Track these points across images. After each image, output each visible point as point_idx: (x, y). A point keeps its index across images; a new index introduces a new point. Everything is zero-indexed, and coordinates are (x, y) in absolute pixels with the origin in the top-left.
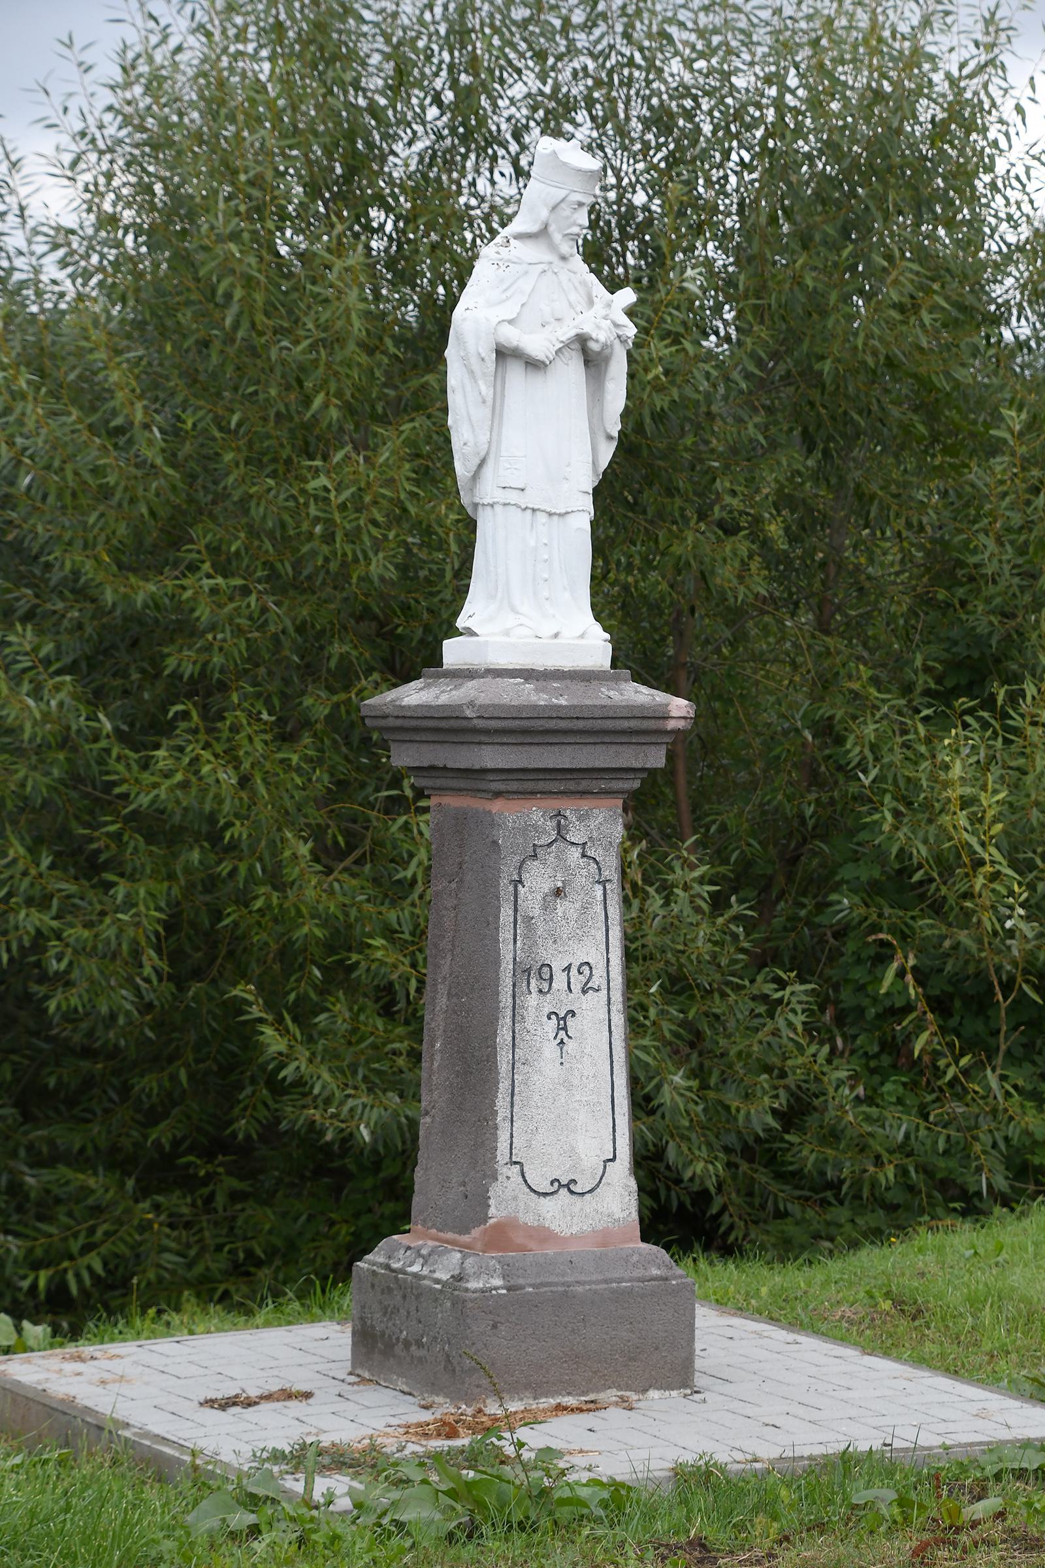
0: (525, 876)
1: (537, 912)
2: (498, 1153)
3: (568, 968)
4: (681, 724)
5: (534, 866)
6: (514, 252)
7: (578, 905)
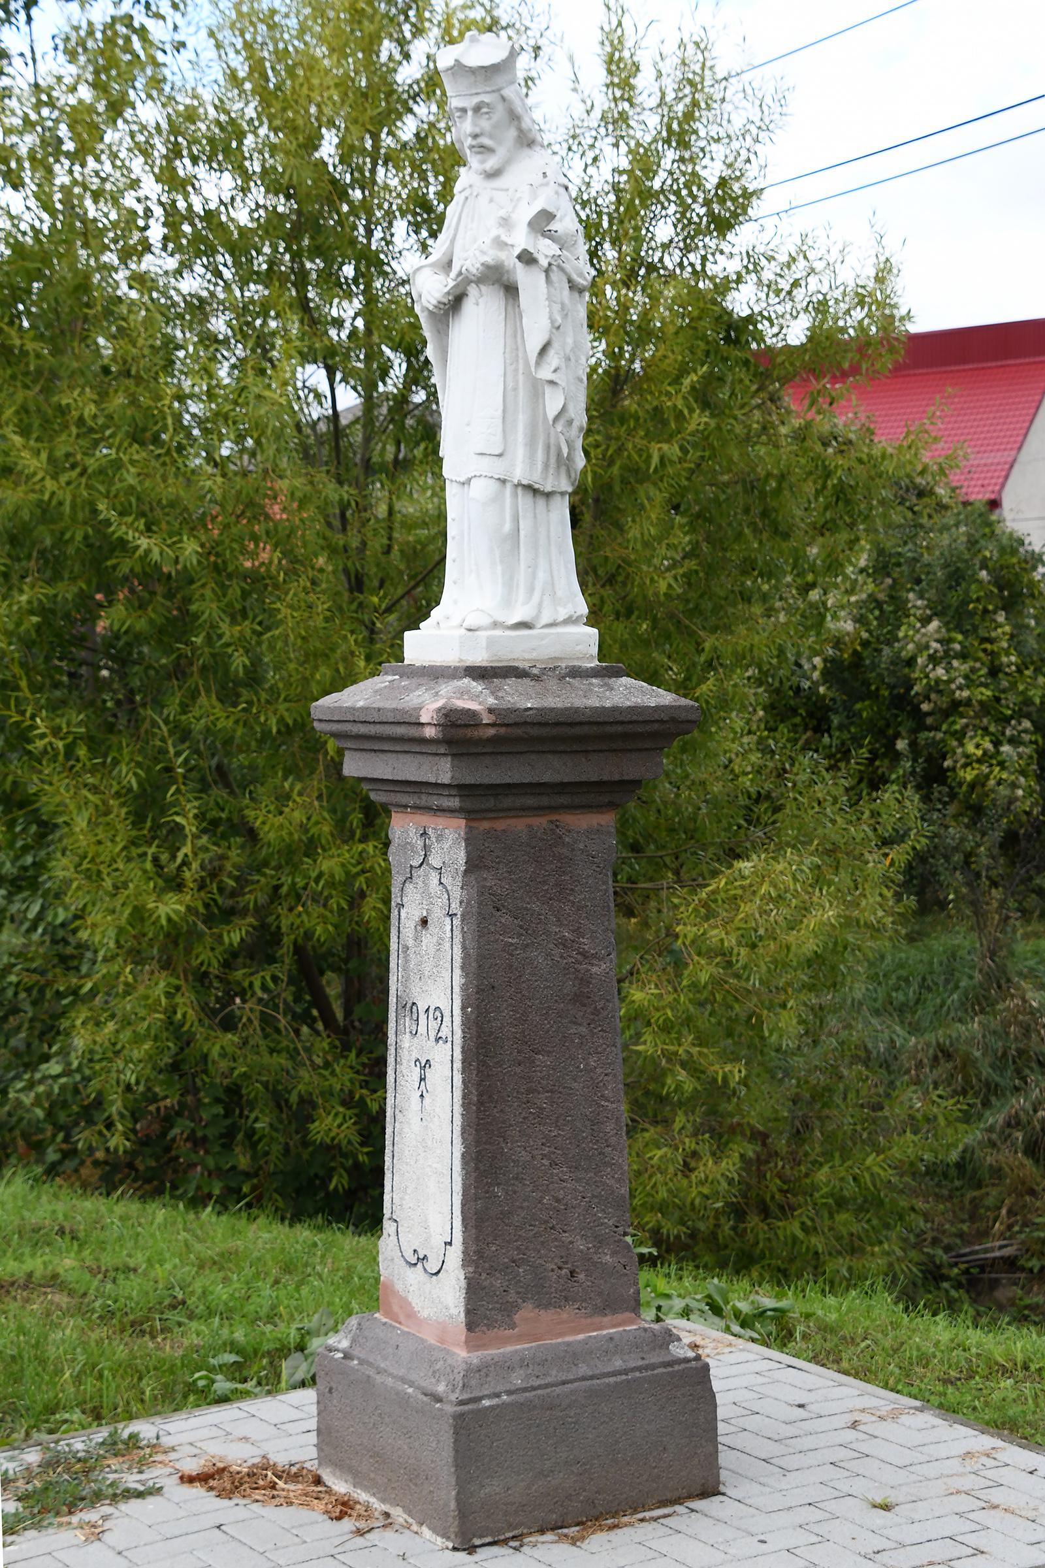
5: (409, 887)
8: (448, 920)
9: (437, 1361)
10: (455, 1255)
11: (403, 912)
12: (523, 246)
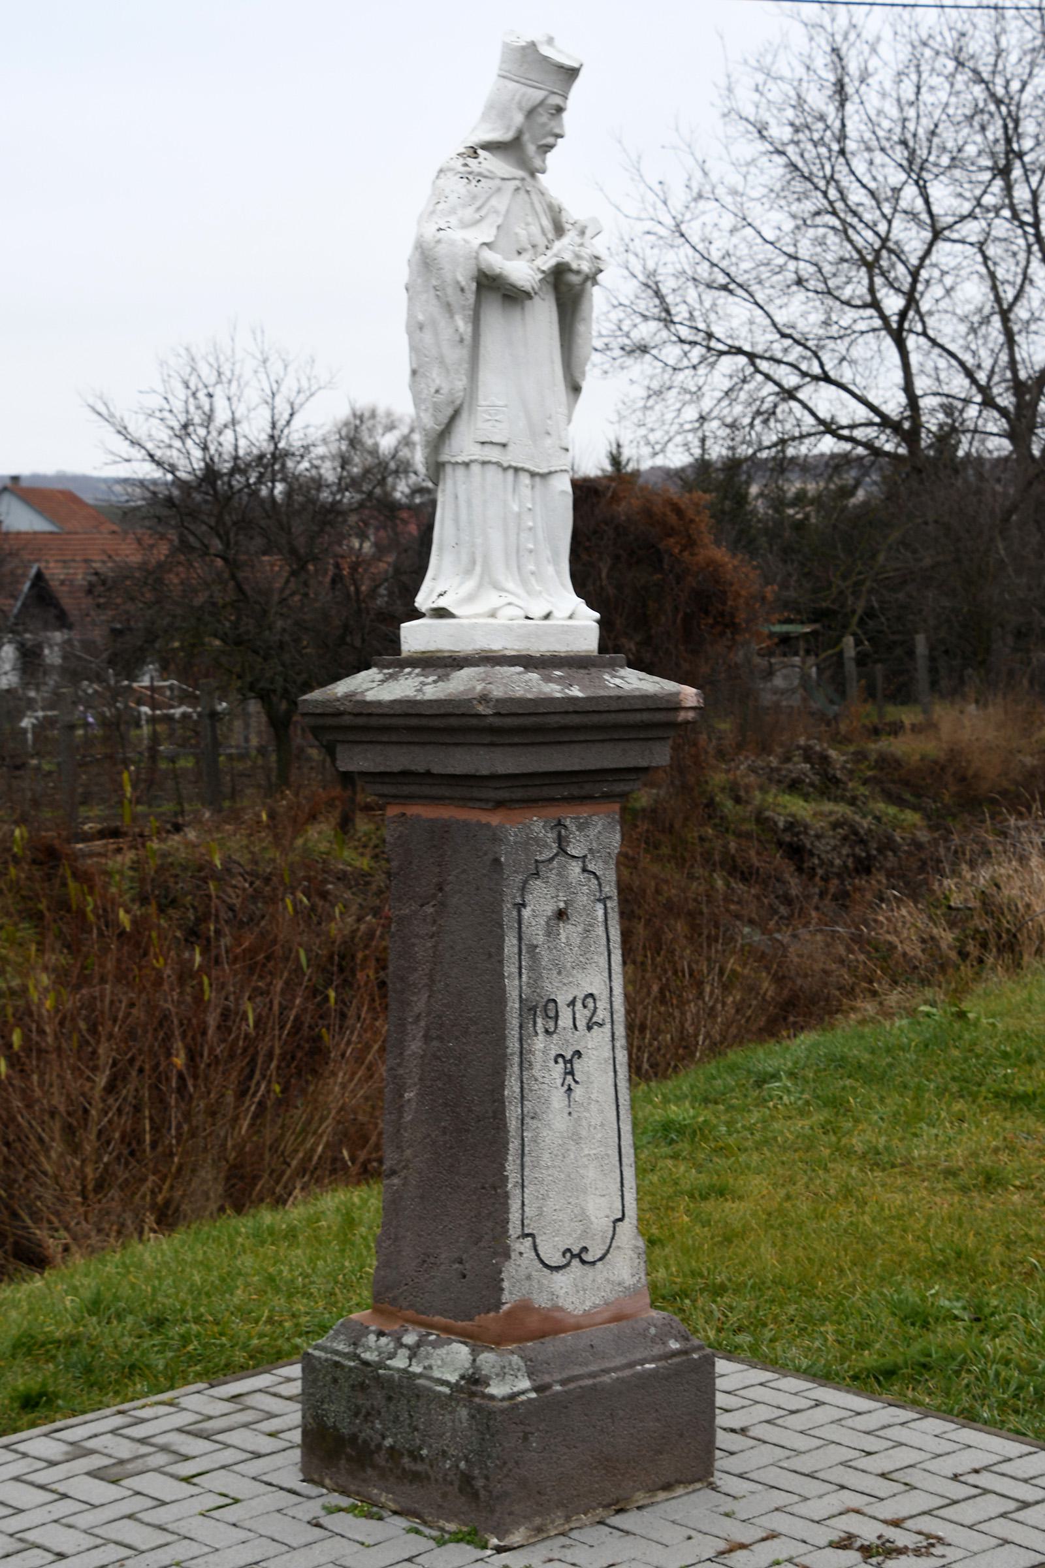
0: (529, 897)
1: (541, 939)
2: (510, 1226)
3: (572, 1003)
4: (691, 715)
6: (485, 165)
7: (580, 929)
8: (600, 906)
10: (628, 1229)
11: (526, 913)
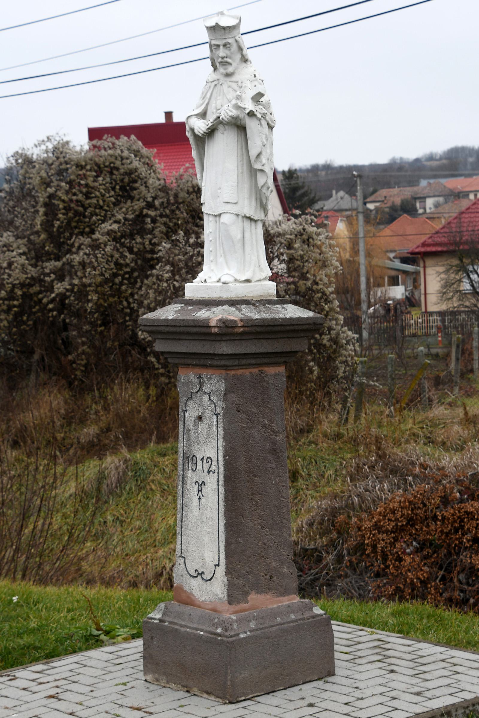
0: (188, 408)
3: (202, 459)
5: (190, 402)
7: (207, 426)
8: (215, 417)
9: (214, 619)
10: (221, 571)
11: (187, 414)
12: (251, 109)
